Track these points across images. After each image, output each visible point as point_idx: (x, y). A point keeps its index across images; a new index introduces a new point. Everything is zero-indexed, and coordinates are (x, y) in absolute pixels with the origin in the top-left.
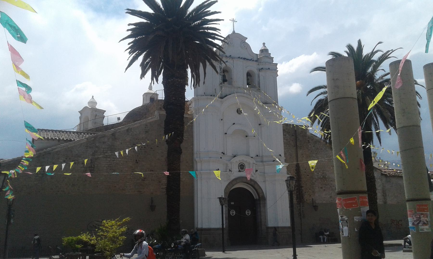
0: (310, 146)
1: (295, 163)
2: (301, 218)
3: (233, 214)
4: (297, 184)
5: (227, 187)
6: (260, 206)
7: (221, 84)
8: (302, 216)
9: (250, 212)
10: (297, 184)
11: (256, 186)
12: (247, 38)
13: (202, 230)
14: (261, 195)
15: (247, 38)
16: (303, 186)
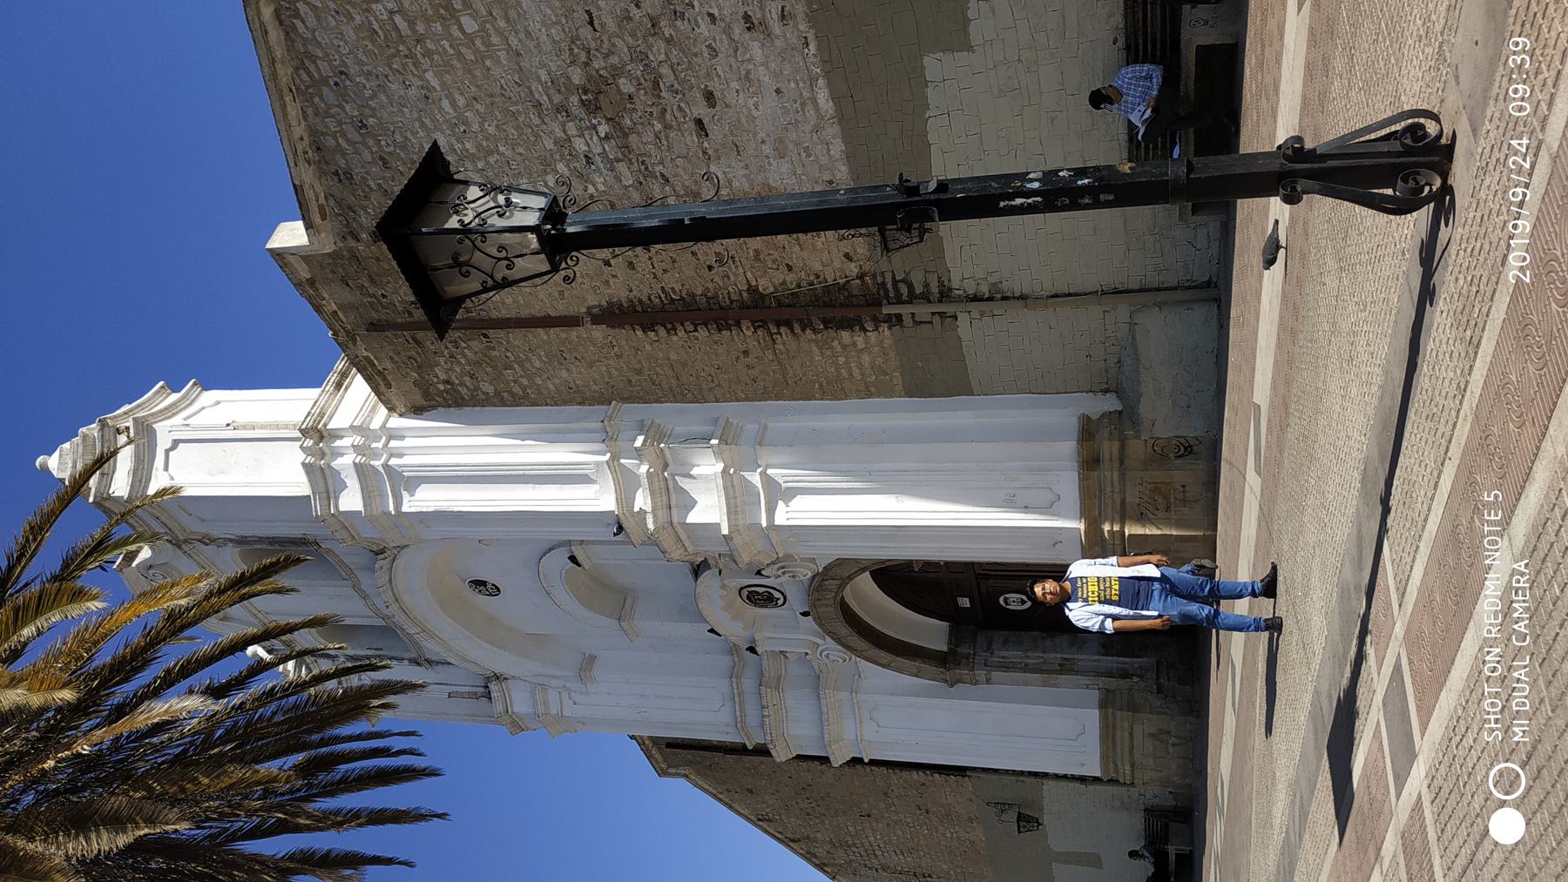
1: (599, 332)
10: (745, 324)
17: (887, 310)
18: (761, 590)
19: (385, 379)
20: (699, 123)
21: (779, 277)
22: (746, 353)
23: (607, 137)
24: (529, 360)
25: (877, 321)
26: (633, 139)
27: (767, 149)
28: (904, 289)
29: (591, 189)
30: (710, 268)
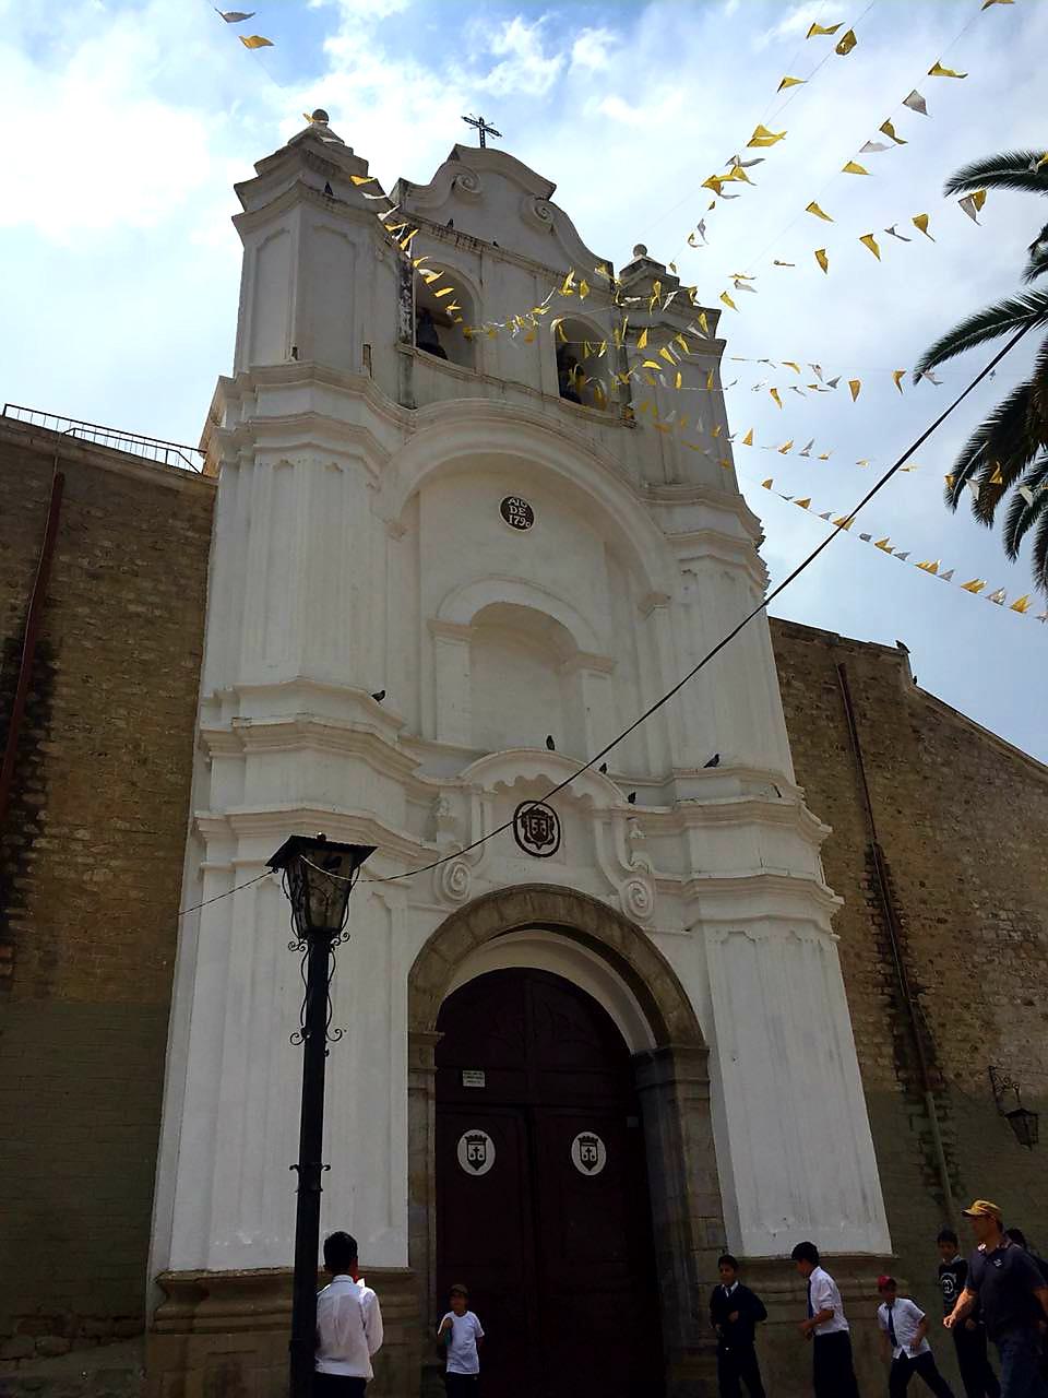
0: (927, 758)
1: (859, 840)
2: (940, 1199)
3: (477, 1164)
4: (889, 970)
5: (431, 946)
6: (673, 1101)
7: (406, 340)
8: (948, 1182)
9: (600, 1153)
10: (889, 970)
11: (637, 958)
12: (553, 187)
13: (199, 1288)
14: (672, 1018)
15: (553, 187)
16: (920, 980)
17: (930, 1095)
18: (555, 832)
19: (790, 636)
20: (1031, 1003)
21: (933, 1010)
22: (858, 955)
23: (1010, 936)
24: (826, 768)
25: (906, 1082)
26: (1010, 953)
27: (1024, 1042)
28: (941, 1113)
29: (977, 906)
30: (931, 962)
